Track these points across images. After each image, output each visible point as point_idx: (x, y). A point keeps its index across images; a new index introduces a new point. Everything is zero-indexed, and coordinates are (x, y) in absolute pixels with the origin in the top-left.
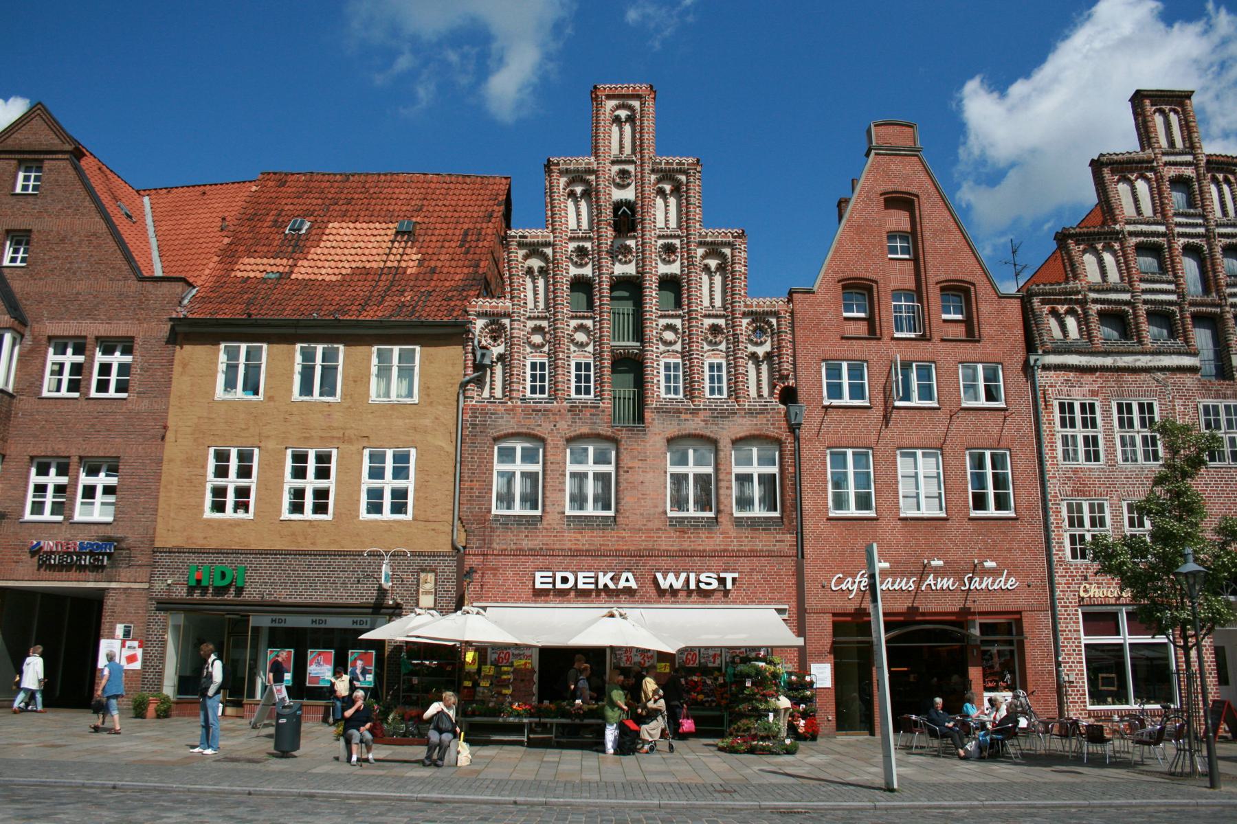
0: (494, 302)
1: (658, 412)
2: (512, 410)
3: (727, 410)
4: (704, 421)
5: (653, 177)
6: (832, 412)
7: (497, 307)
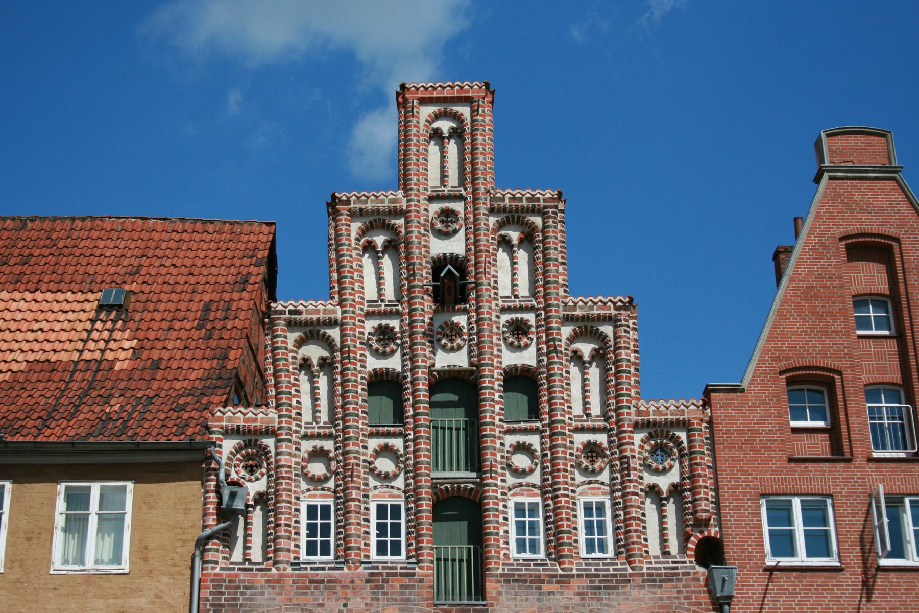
0: (250, 412)
1: (507, 581)
2: (278, 581)
3: (615, 576)
4: (579, 594)
5: (492, 220)
6: (782, 579)
7: (255, 420)
